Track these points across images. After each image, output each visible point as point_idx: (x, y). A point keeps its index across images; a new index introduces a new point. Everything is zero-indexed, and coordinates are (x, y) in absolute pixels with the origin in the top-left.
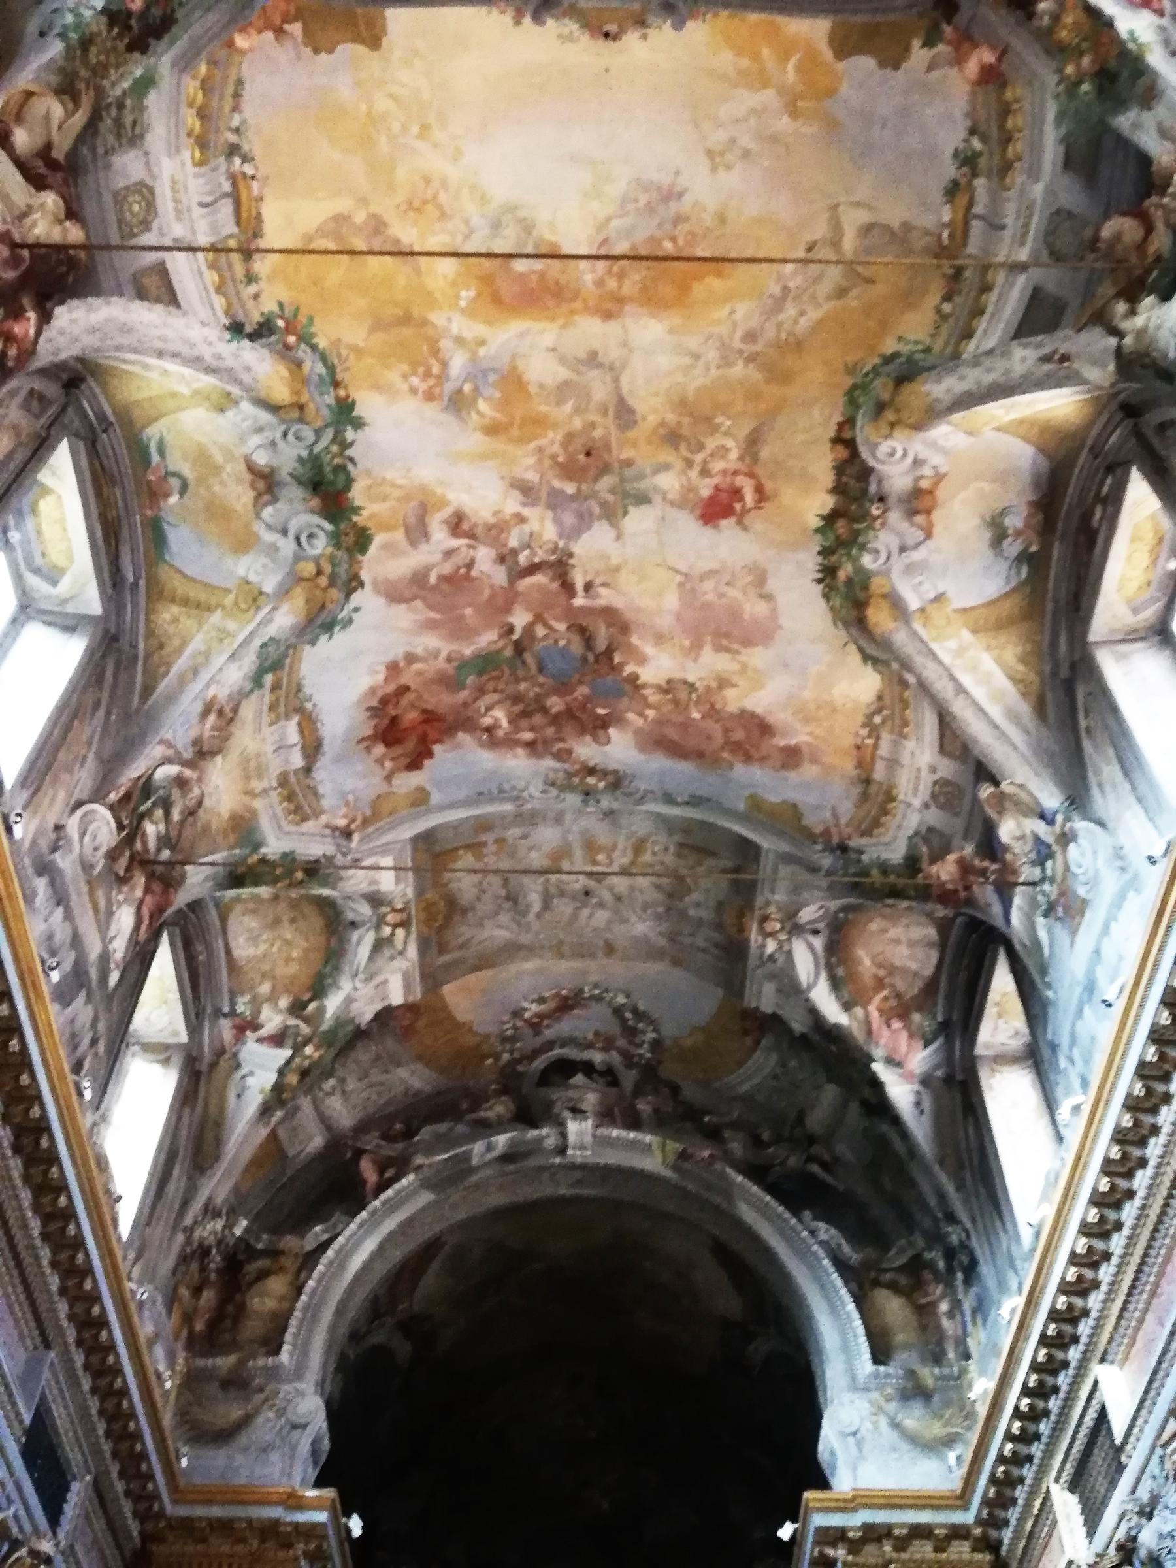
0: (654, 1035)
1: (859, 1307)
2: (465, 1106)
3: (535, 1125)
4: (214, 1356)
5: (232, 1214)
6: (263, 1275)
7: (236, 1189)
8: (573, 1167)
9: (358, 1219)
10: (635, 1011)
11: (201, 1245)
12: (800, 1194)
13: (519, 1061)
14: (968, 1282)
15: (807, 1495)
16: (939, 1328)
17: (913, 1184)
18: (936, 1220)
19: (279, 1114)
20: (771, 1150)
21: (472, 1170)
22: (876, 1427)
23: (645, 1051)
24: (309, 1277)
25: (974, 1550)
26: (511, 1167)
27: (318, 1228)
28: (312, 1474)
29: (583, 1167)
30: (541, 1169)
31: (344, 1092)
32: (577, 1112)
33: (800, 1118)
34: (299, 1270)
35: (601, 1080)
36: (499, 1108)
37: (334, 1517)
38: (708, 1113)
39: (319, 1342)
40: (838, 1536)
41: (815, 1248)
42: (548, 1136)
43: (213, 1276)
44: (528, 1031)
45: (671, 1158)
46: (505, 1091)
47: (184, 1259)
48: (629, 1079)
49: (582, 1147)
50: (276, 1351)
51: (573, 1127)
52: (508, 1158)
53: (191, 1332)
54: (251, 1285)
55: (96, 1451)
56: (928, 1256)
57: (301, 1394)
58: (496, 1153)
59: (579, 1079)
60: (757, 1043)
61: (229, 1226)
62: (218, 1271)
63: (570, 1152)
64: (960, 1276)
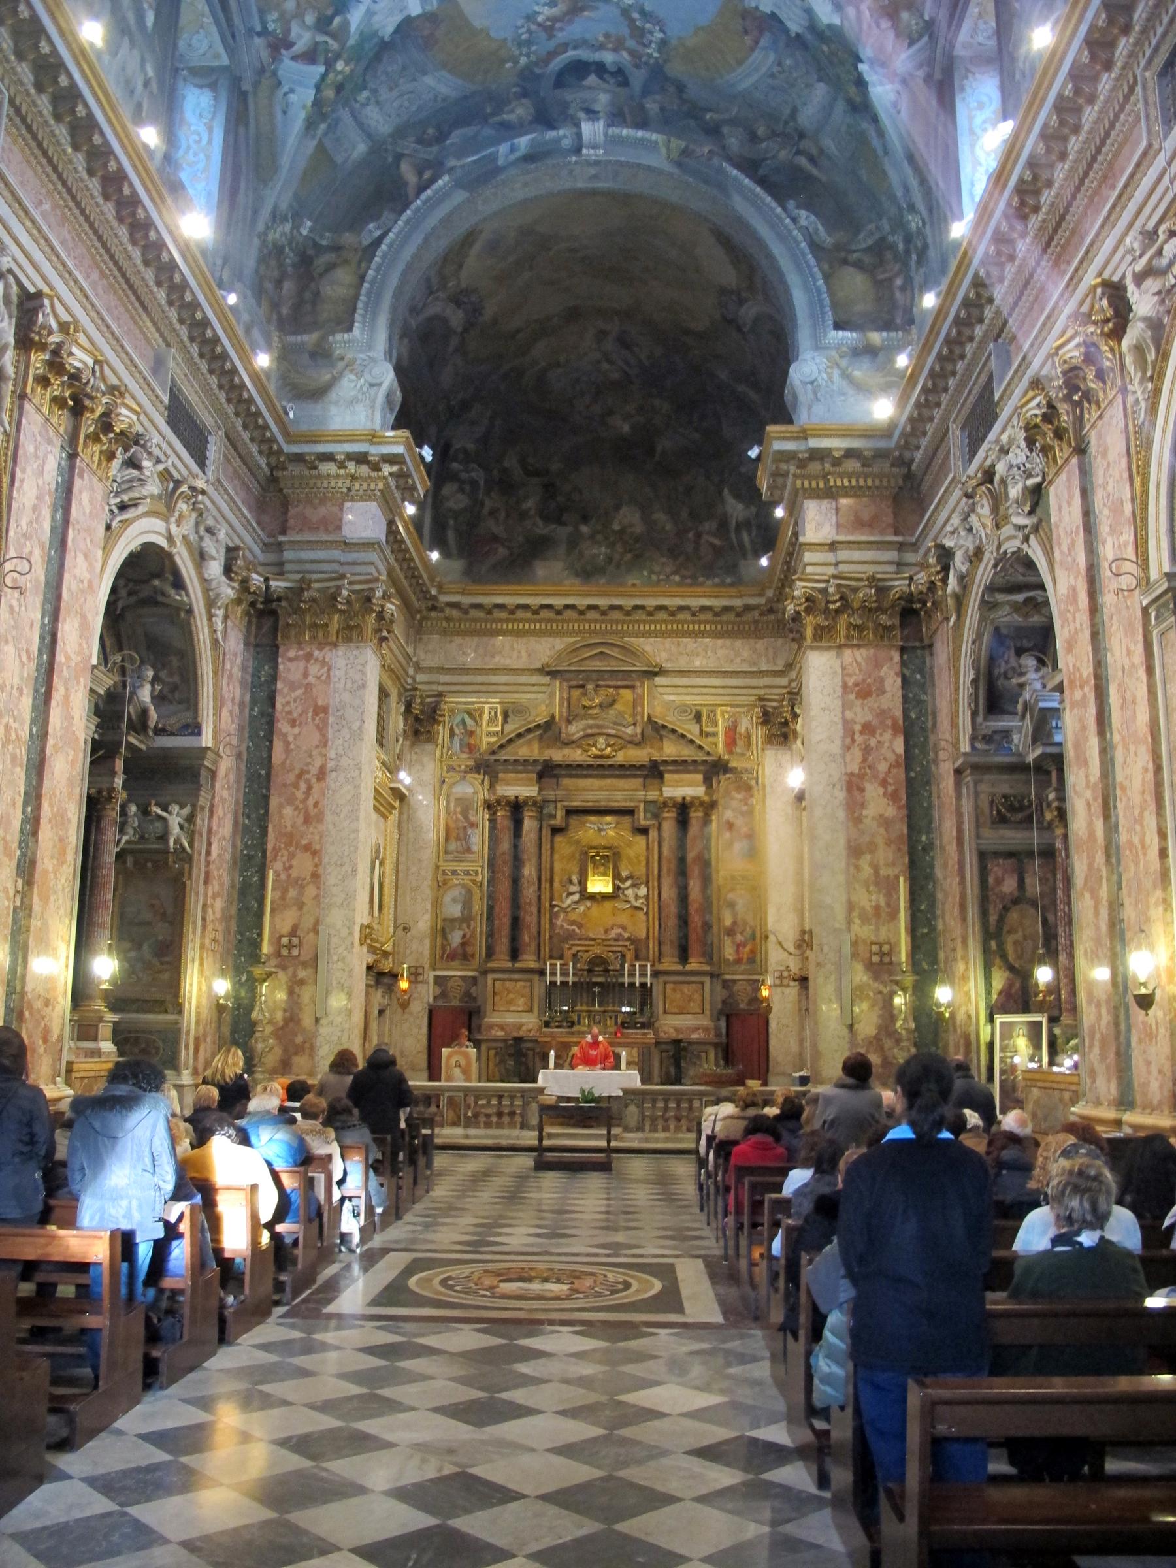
0: (661, 35)
1: (826, 283)
2: (489, 110)
3: (553, 128)
4: (300, 333)
5: (297, 217)
6: (331, 267)
7: (296, 196)
8: (589, 164)
9: (404, 217)
10: (643, 12)
11: (275, 245)
12: (785, 184)
13: (536, 64)
14: (919, 262)
15: (769, 428)
17: (884, 173)
18: (900, 208)
19: (323, 126)
20: (764, 145)
21: (498, 170)
23: (652, 51)
24: (368, 268)
25: (893, 465)
27: (371, 226)
28: (391, 419)
31: (378, 103)
32: (592, 114)
33: (794, 112)
34: (360, 262)
35: (612, 81)
36: (521, 111)
37: (409, 449)
38: (710, 110)
40: (789, 456)
41: (795, 232)
42: (565, 136)
43: (290, 269)
44: (543, 35)
45: (675, 155)
46: (525, 94)
48: (638, 78)
49: (595, 147)
50: (350, 329)
51: (587, 128)
52: (530, 158)
54: (321, 275)
55: (221, 412)
58: (518, 154)
59: (592, 79)
60: (757, 42)
61: (296, 227)
62: (293, 265)
63: (584, 151)
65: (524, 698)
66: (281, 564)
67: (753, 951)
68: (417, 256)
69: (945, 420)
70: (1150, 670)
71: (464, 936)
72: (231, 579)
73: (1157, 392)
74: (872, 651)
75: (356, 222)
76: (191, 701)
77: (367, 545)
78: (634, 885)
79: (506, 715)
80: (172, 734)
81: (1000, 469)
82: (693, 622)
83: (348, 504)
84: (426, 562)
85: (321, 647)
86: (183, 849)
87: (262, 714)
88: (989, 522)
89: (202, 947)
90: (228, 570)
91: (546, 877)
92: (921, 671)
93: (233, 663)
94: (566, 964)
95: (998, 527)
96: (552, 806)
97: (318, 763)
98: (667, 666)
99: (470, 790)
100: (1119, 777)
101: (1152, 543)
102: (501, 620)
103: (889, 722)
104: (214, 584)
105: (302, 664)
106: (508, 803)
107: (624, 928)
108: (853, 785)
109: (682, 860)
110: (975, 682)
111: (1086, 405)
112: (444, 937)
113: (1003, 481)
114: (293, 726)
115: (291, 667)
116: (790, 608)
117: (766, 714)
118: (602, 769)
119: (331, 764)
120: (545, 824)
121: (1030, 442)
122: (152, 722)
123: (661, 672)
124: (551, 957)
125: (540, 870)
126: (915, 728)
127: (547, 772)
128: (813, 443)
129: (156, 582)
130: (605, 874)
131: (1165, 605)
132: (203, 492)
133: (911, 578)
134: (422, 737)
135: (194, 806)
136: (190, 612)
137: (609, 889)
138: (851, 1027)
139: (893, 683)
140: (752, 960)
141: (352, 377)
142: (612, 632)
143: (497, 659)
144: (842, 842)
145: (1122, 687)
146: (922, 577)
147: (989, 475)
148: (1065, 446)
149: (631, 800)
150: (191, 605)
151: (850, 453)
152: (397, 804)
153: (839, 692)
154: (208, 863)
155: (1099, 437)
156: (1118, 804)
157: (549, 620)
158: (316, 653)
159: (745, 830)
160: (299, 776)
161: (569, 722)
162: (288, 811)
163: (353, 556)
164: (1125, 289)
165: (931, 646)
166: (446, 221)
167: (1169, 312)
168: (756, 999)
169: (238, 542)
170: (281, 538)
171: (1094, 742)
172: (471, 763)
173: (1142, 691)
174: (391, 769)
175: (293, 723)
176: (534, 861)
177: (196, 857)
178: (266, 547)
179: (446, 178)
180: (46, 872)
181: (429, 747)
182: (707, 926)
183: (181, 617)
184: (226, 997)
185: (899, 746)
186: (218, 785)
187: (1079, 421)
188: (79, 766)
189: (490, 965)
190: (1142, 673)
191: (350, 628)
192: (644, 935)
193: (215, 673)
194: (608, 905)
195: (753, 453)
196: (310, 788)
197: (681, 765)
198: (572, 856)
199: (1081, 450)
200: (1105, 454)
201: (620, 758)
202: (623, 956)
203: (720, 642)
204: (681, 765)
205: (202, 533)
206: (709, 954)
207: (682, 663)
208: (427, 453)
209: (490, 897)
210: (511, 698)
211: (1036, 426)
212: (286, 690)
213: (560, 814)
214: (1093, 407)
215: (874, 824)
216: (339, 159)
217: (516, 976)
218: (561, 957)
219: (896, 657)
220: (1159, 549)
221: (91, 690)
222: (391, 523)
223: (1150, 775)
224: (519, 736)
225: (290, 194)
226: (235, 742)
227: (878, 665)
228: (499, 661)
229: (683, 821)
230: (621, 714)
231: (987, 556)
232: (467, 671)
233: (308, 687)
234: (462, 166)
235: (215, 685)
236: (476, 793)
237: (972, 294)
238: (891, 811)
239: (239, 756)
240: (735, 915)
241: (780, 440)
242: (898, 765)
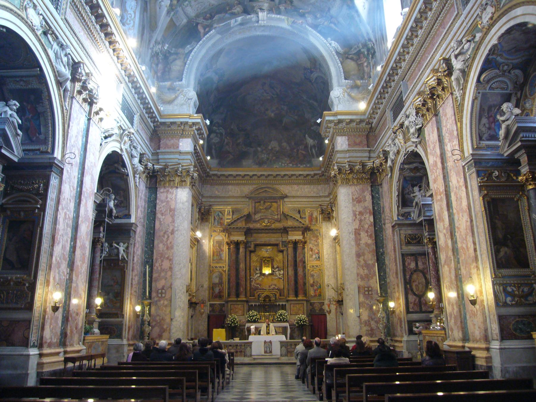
5: (163, 43)
6: (175, 60)
7: (163, 36)
9: (199, 43)
11: (156, 52)
16: (364, 70)
22: (344, 96)
26: (243, 27)
27: (188, 46)
28: (195, 110)
29: (264, 26)
30: (251, 27)
34: (185, 58)
37: (202, 121)
39: (192, 77)
47: (152, 57)
50: (181, 80)
53: (157, 77)
54: (171, 63)
56: (362, 50)
57: (189, 91)
61: (163, 46)
64: (371, 56)
65: (239, 206)
66: (158, 160)
67: (320, 292)
68: (204, 57)
69: (386, 106)
70: (466, 187)
72: (141, 164)
73: (464, 94)
74: (361, 186)
75: (183, 46)
76: (127, 206)
77: (187, 153)
78: (279, 270)
79: (233, 212)
80: (121, 218)
81: (406, 123)
83: (181, 139)
84: (206, 159)
85: (172, 187)
86: (125, 259)
87: (151, 211)
88: (402, 141)
89: (131, 294)
90: (140, 162)
91: (248, 268)
92: (378, 193)
93: (142, 193)
95: (405, 143)
97: (171, 228)
99: (221, 238)
100: (456, 225)
101: (465, 144)
102: (231, 180)
103: (368, 211)
104: (136, 166)
105: (165, 194)
106: (235, 243)
107: (275, 285)
108: (357, 233)
109: (295, 261)
110: (398, 196)
111: (438, 99)
112: (213, 289)
113: (407, 128)
114: (162, 215)
115: (161, 195)
116: (333, 173)
117: (322, 210)
118: (268, 230)
119: (176, 229)
121: (417, 113)
122: (114, 215)
123: (286, 197)
126: (377, 213)
127: (248, 232)
128: (339, 117)
129: (116, 165)
130: (268, 267)
131: (471, 164)
132: (133, 134)
133: (374, 162)
135: (128, 243)
136: (128, 175)
137: (270, 272)
138: (359, 317)
139: (369, 198)
141: (182, 96)
142: (270, 184)
143: (230, 193)
144: (354, 252)
145: (456, 194)
146: (377, 162)
147: (402, 125)
148: (430, 114)
149: (277, 241)
150: (128, 173)
151: (352, 121)
152: (196, 243)
153: (351, 201)
154: (133, 264)
155: (443, 110)
156: (456, 234)
157: (247, 180)
158: (170, 190)
159: (316, 251)
160: (165, 233)
161: (255, 214)
162: (161, 245)
163: (182, 157)
164: (451, 60)
165: (381, 184)
166: (214, 45)
167: (467, 67)
168: (322, 310)
169: (144, 152)
170: (158, 151)
171: (446, 213)
172: (221, 229)
173: (464, 194)
174: (194, 230)
175: (162, 214)
176: (244, 263)
177: (129, 262)
178: (153, 154)
179: (214, 30)
180: (78, 266)
181: (207, 223)
182: (305, 284)
183: (124, 177)
184: (139, 312)
185: (372, 220)
186: (137, 236)
187: (435, 105)
188: (90, 228)
190: (464, 188)
191: (182, 181)
192: (282, 287)
193: (136, 197)
194: (270, 278)
195: (319, 121)
196: (168, 237)
197: (295, 229)
198: (257, 260)
199: (436, 115)
200: (446, 115)
201: (273, 226)
202: (276, 295)
203: (306, 186)
204: (295, 229)
205: (132, 148)
206: (305, 294)
207: (293, 194)
208: (208, 122)
209: (228, 275)
211: (419, 108)
212: (160, 203)
213: (252, 246)
214: (441, 100)
215: (364, 246)
216: (177, 24)
217: (238, 303)
219: (370, 189)
220: (468, 146)
221: (95, 202)
222: (195, 146)
223: (469, 223)
224: (238, 219)
225: (161, 35)
226: (142, 221)
227: (363, 192)
228: (230, 194)
229: (295, 249)
230: (273, 211)
231: (401, 153)
232: (220, 197)
233: (168, 202)
234: (219, 27)
235: (136, 201)
236: (223, 239)
237: (394, 65)
238: (370, 241)
239: (144, 226)
240: (314, 279)
241: (328, 117)
242: (371, 226)
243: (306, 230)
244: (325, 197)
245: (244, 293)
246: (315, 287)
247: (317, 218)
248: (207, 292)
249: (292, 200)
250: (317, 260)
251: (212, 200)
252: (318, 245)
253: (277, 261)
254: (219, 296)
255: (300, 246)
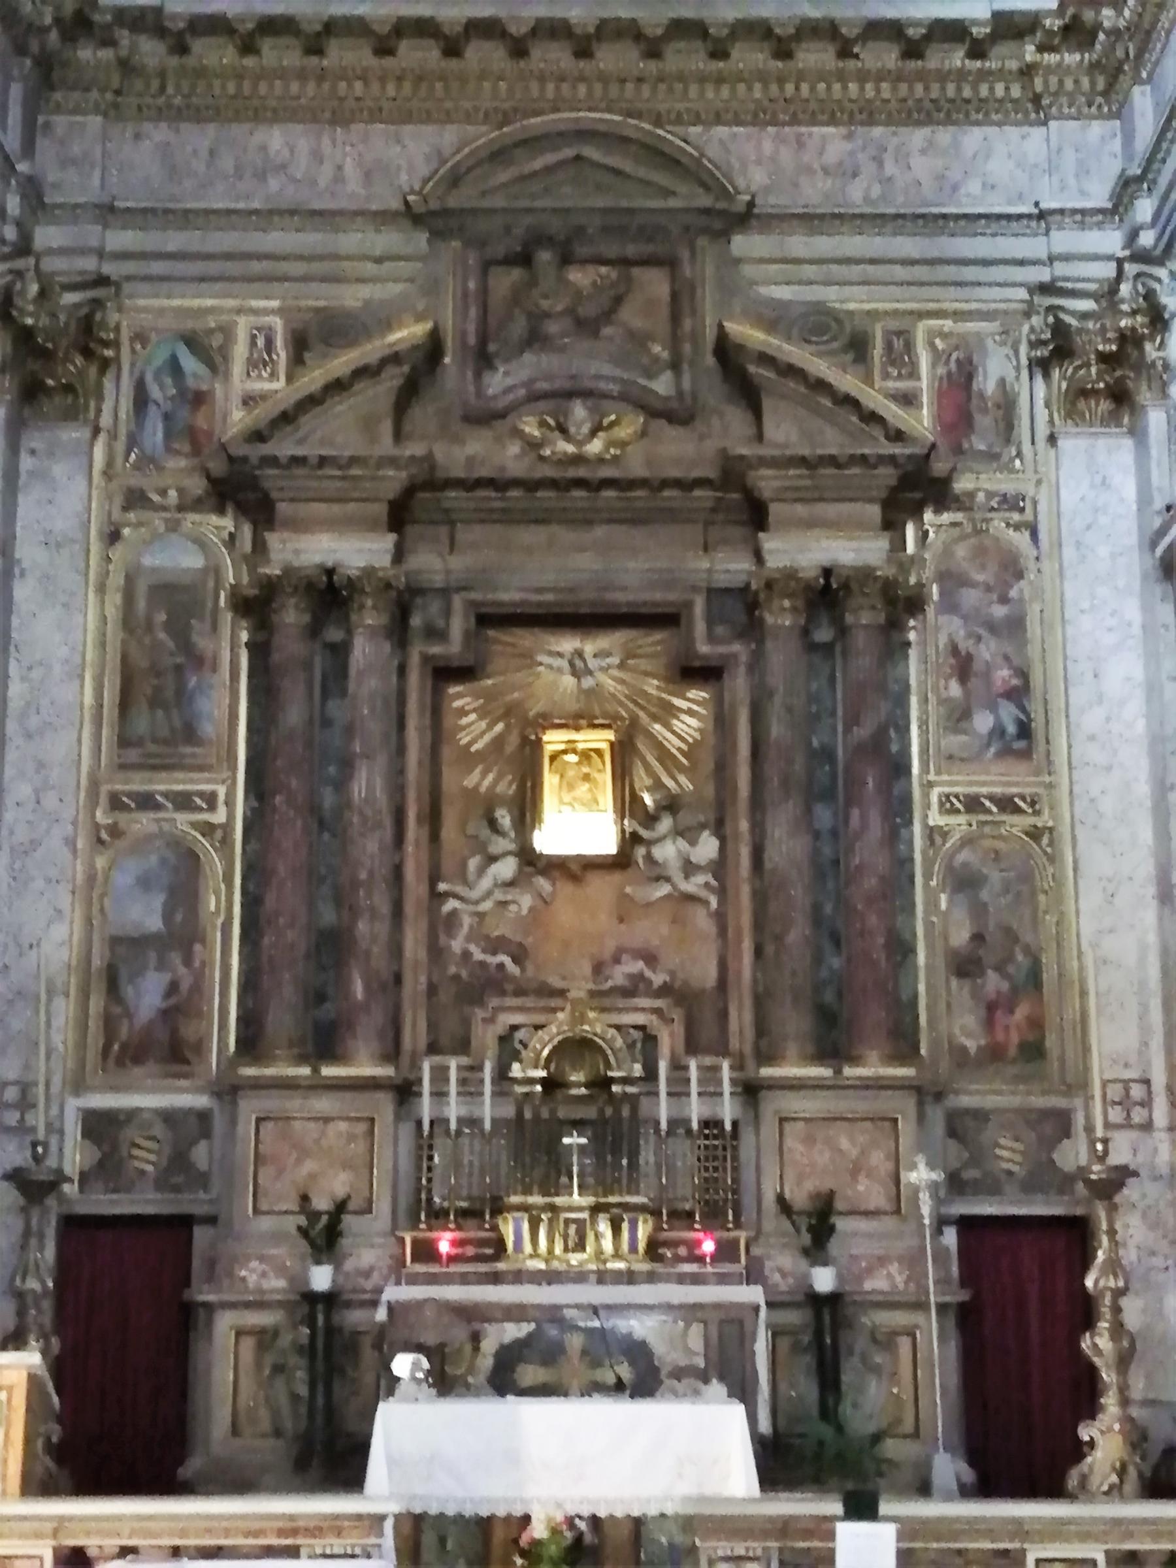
71: (173, 988)
78: (679, 832)
79: (300, 346)
82: (842, 77)
94: (478, 1068)
96: (435, 607)
98: (768, 203)
99: (193, 560)
117: (1060, 330)
120: (415, 659)
123: (746, 218)
124: (433, 1048)
125: (397, 790)
134: (47, 406)
140: (1033, 1051)
143: (274, 184)
149: (669, 585)
181: (74, 434)
189: (249, 1071)
192: (706, 973)
194: (601, 887)
202: (650, 1040)
206: (903, 1043)
207: (814, 193)
210: (318, 297)
213: (458, 626)
218: (463, 1046)
236: (216, 571)
240: (979, 911)
243: (917, 487)
244: (1083, 217)
245: (377, 1017)
246: (993, 982)
247: (1007, 406)
248: (64, 1011)
249: (798, 244)
250: (1006, 752)
251: (121, 239)
252: (1015, 626)
253: (664, 755)
254: (167, 1046)
255: (864, 616)
